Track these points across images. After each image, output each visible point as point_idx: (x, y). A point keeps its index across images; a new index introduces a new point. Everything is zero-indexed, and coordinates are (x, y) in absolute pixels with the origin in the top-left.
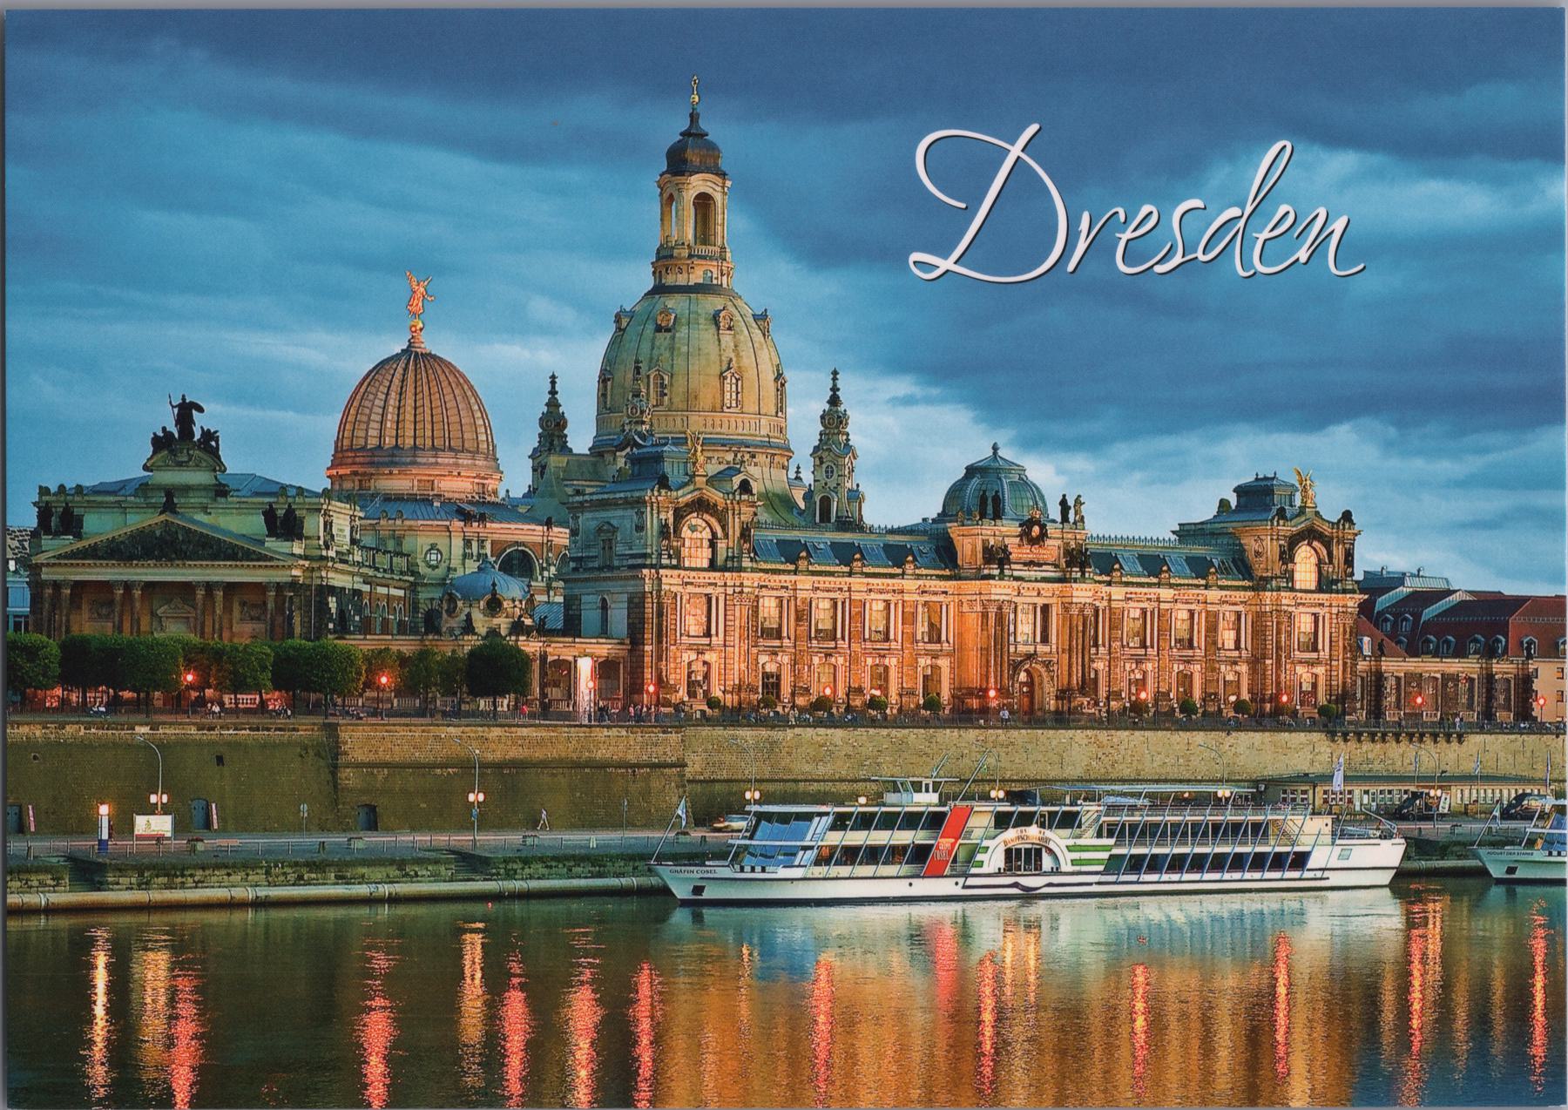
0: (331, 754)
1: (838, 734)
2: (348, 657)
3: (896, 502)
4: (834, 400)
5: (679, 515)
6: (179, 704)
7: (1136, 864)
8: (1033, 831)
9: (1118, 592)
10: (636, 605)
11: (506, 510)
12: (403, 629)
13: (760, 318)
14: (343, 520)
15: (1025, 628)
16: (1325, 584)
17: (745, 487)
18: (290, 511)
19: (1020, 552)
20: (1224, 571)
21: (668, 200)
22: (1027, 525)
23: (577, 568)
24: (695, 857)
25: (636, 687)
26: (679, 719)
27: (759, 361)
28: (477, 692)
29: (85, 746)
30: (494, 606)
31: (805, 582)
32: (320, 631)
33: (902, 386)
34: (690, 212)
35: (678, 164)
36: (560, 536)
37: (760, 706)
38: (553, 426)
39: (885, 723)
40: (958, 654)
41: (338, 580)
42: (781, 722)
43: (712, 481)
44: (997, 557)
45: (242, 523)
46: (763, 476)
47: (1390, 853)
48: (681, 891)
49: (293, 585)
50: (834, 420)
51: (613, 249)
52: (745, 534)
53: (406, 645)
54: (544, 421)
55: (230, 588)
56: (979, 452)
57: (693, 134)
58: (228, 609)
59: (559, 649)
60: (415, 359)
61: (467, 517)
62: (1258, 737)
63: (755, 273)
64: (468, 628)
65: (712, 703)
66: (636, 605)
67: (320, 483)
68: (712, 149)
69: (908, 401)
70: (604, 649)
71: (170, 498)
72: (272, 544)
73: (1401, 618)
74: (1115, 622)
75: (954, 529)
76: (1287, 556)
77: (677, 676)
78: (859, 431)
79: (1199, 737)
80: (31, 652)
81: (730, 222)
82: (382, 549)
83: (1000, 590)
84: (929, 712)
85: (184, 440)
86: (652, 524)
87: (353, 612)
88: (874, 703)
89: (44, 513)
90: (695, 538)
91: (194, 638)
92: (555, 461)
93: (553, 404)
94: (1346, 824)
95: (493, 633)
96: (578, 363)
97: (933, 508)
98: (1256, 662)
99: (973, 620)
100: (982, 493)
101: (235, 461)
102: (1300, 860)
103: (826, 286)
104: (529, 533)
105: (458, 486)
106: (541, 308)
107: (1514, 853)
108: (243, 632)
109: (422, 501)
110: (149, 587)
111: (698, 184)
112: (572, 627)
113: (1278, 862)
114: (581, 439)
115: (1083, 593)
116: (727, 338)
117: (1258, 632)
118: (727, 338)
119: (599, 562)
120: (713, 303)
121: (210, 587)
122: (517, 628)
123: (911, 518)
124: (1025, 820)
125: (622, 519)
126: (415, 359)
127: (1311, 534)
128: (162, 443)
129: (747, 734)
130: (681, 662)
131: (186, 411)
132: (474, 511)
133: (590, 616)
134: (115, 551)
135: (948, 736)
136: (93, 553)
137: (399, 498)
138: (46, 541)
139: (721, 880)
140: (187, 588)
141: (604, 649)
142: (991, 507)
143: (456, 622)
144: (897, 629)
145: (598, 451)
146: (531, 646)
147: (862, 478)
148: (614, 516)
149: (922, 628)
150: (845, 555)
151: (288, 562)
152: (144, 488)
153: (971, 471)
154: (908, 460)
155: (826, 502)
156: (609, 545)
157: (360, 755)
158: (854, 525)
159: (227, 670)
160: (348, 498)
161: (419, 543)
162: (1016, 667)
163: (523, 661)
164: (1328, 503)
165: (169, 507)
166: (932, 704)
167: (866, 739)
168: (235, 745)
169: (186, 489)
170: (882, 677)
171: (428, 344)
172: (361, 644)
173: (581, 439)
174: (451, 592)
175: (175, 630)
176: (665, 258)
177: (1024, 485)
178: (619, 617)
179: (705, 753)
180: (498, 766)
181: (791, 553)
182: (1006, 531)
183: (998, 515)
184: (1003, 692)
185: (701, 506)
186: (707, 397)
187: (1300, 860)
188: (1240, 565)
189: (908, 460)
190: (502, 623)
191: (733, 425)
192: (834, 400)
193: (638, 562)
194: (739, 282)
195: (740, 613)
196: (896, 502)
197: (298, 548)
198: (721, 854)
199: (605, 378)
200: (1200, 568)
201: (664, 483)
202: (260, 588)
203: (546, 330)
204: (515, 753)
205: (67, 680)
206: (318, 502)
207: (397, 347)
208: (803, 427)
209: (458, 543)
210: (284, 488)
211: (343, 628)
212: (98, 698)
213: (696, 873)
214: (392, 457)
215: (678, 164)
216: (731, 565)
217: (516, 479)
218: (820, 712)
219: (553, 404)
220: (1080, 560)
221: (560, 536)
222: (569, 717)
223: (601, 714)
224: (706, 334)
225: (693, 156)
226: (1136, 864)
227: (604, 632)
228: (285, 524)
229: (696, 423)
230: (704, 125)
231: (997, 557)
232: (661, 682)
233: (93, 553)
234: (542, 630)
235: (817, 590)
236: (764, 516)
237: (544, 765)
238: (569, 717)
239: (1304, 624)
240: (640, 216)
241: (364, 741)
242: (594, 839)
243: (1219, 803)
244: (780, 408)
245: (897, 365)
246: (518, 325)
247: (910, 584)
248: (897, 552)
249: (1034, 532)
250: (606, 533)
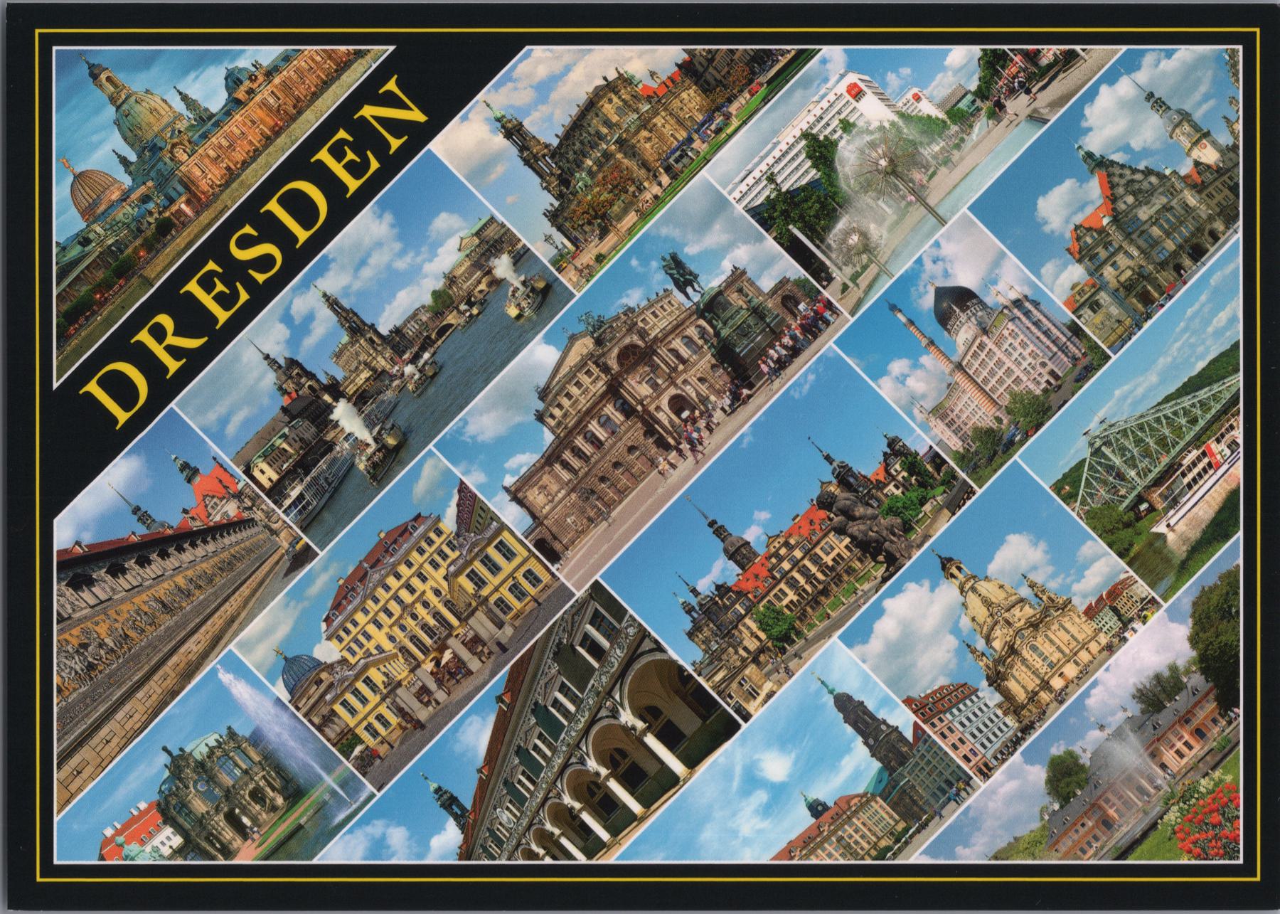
2: (129, 256)
3: (216, 101)
4: (180, 93)
5: (171, 152)
6: (102, 304)
9: (285, 73)
11: (131, 190)
12: (135, 238)
13: (147, 91)
15: (271, 101)
17: (180, 132)
19: (255, 86)
22: (250, 78)
25: (199, 200)
26: (216, 197)
27: (156, 102)
28: (165, 236)
30: (151, 213)
31: (213, 139)
33: (192, 75)
34: (108, 85)
35: (95, 77)
36: (150, 184)
37: (231, 176)
38: (124, 161)
40: (262, 121)
41: (110, 242)
42: (239, 175)
43: (171, 138)
44: (251, 92)
45: (75, 252)
46: (182, 126)
50: (184, 98)
51: (98, 110)
52: (190, 142)
53: (138, 242)
55: (87, 268)
56: (223, 73)
57: (91, 67)
59: (174, 208)
60: (79, 177)
61: (125, 200)
63: (136, 83)
64: (150, 224)
66: (181, 182)
67: (84, 225)
69: (197, 77)
70: (184, 198)
74: (290, 78)
77: (206, 188)
78: (193, 94)
79: (334, 86)
81: (121, 77)
82: (112, 227)
83: (258, 98)
84: (268, 141)
86: (167, 160)
88: (255, 151)
92: (132, 168)
93: (119, 156)
96: (116, 141)
97: (225, 95)
99: (259, 111)
100: (233, 81)
103: (155, 71)
104: (142, 189)
105: (115, 196)
106: (95, 138)
108: (100, 275)
109: (111, 206)
110: (69, 285)
111: (103, 77)
112: (172, 201)
114: (133, 157)
115: (277, 81)
116: (144, 104)
119: (163, 181)
120: (132, 99)
121: (82, 272)
122: (160, 213)
123: (223, 102)
125: (160, 165)
126: (79, 177)
129: (235, 185)
130: (204, 185)
132: (125, 197)
133: (174, 194)
135: (278, 140)
137: (106, 210)
140: (78, 276)
142: (239, 82)
143: (146, 225)
144: (244, 130)
145: (139, 157)
146: (167, 214)
147: (204, 104)
150: (217, 124)
151: (94, 250)
154: (209, 89)
155: (201, 118)
158: (212, 116)
159: (105, 286)
160: (94, 222)
161: (120, 216)
162: (278, 111)
163: (168, 218)
166: (268, 138)
167: (262, 160)
170: (251, 143)
171: (78, 170)
172: (130, 250)
173: (133, 157)
174: (138, 220)
175: (84, 289)
176: (112, 100)
177: (241, 70)
178: (180, 188)
181: (205, 136)
182: (247, 83)
183: (241, 82)
185: (174, 146)
186: (152, 120)
189: (209, 89)
190: (156, 215)
191: (165, 120)
192: (180, 93)
193: (172, 173)
194: (134, 88)
195: (207, 161)
196: (216, 101)
201: (161, 149)
202: (94, 261)
203: (100, 143)
205: (71, 324)
207: (71, 178)
208: (179, 106)
211: (122, 252)
212: (82, 320)
214: (95, 204)
215: (95, 77)
217: (127, 181)
218: (245, 164)
219: (119, 156)
220: (269, 74)
221: (150, 184)
222: (191, 221)
224: (138, 108)
225: (96, 71)
227: (180, 195)
228: (85, 242)
229: (156, 129)
230: (92, 62)
231: (251, 92)
232: (204, 193)
234: (166, 208)
235: (218, 139)
236: (190, 134)
240: (99, 97)
245: (186, 72)
246: (95, 146)
247: (237, 117)
248: (228, 112)
249: (252, 78)
250: (159, 172)
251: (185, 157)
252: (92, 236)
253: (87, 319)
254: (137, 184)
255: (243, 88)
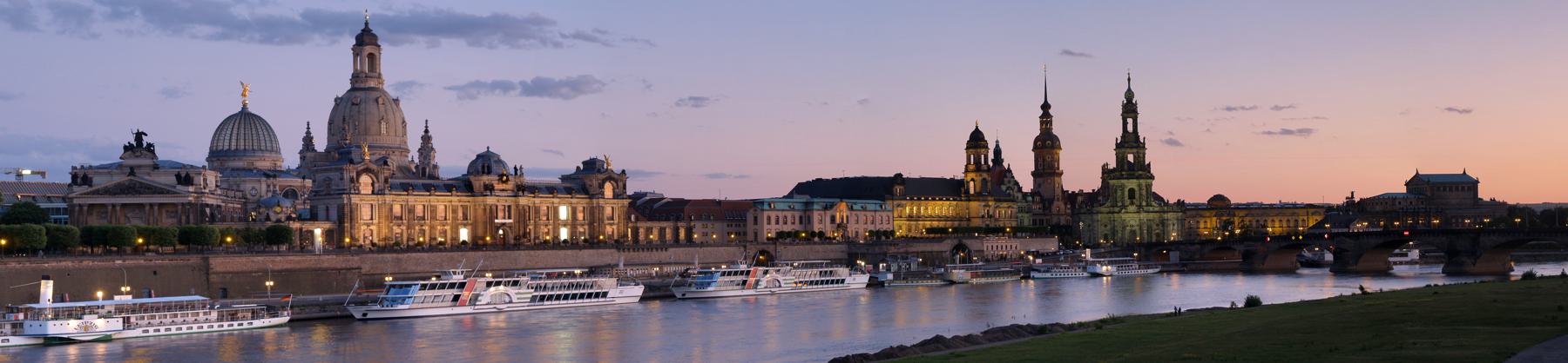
0: (206, 269)
1: (425, 255)
5: (359, 174)
6: (137, 250)
7: (542, 298)
8: (502, 288)
9: (537, 201)
10: (341, 208)
14: (212, 178)
16: (616, 196)
18: (187, 175)
19: (498, 186)
20: (578, 192)
21: (356, 55)
23: (315, 194)
24: (363, 303)
25: (341, 239)
28: (271, 243)
29: (92, 269)
31: (411, 198)
32: (203, 221)
36: (309, 183)
38: (308, 140)
39: (446, 250)
41: (210, 201)
45: (168, 179)
47: (639, 290)
48: (358, 316)
49: (190, 203)
52: (386, 181)
54: (304, 139)
55: (161, 205)
58: (160, 213)
59: (307, 226)
61: (268, 176)
62: (591, 251)
64: (268, 218)
65: (373, 244)
68: (375, 37)
70: (328, 225)
71: (132, 171)
72: (179, 187)
73: (646, 208)
74: (537, 211)
75: (472, 178)
76: (601, 186)
79: (569, 252)
80: (67, 232)
83: (490, 200)
85: (139, 146)
86: (346, 176)
87: (216, 214)
89: (74, 177)
90: (365, 179)
91: (143, 225)
92: (309, 154)
94: (623, 281)
95: (279, 221)
98: (591, 224)
99: (480, 211)
101: (162, 154)
102: (605, 295)
104: (296, 182)
105: (264, 164)
107: (683, 290)
108: (167, 222)
109: (248, 171)
110: (124, 205)
111: (368, 49)
112: (314, 217)
113: (597, 295)
114: (321, 144)
115: (524, 201)
117: (592, 213)
118: (382, 108)
120: (376, 94)
121: (151, 205)
124: (498, 284)
125: (334, 175)
127: (610, 179)
128: (128, 148)
131: (139, 136)
133: (321, 213)
134: (107, 191)
136: (97, 193)
138: (75, 188)
139: (375, 311)
140: (141, 206)
141: (328, 225)
145: (328, 151)
146: (295, 225)
148: (333, 175)
149: (460, 215)
150: (427, 188)
151: (189, 195)
152: (120, 166)
153: (479, 156)
156: (329, 186)
157: (219, 269)
159: (156, 237)
161: (248, 187)
163: (288, 231)
164: (616, 167)
165: (132, 173)
168: (161, 266)
169: (140, 167)
172: (217, 227)
173: (321, 144)
174: (259, 204)
176: (356, 77)
178: (334, 214)
179: (367, 264)
180: (280, 271)
181: (406, 188)
183: (489, 173)
184: (493, 237)
185: (367, 171)
187: (605, 295)
188: (584, 190)
190: (283, 217)
193: (341, 192)
195: (385, 211)
197: (191, 189)
198: (375, 301)
199: (331, 123)
200: (569, 191)
201: (351, 162)
202: (174, 205)
204: (289, 266)
206: (199, 171)
209: (264, 187)
210: (184, 166)
211: (213, 219)
213: (364, 308)
216: (381, 192)
220: (522, 189)
221: (309, 183)
223: (325, 252)
225: (366, 39)
226: (542, 298)
227: (328, 219)
231: (489, 188)
233: (97, 193)
234: (300, 218)
235: (419, 202)
237: (300, 270)
238: (312, 252)
239: (608, 211)
241: (219, 263)
242: (321, 298)
243: (574, 276)
244: (405, 134)
247: (455, 199)
249: (503, 178)
251: (369, 190)
252: (199, 180)
253: (110, 252)
254: (301, 172)
255: (486, 179)
